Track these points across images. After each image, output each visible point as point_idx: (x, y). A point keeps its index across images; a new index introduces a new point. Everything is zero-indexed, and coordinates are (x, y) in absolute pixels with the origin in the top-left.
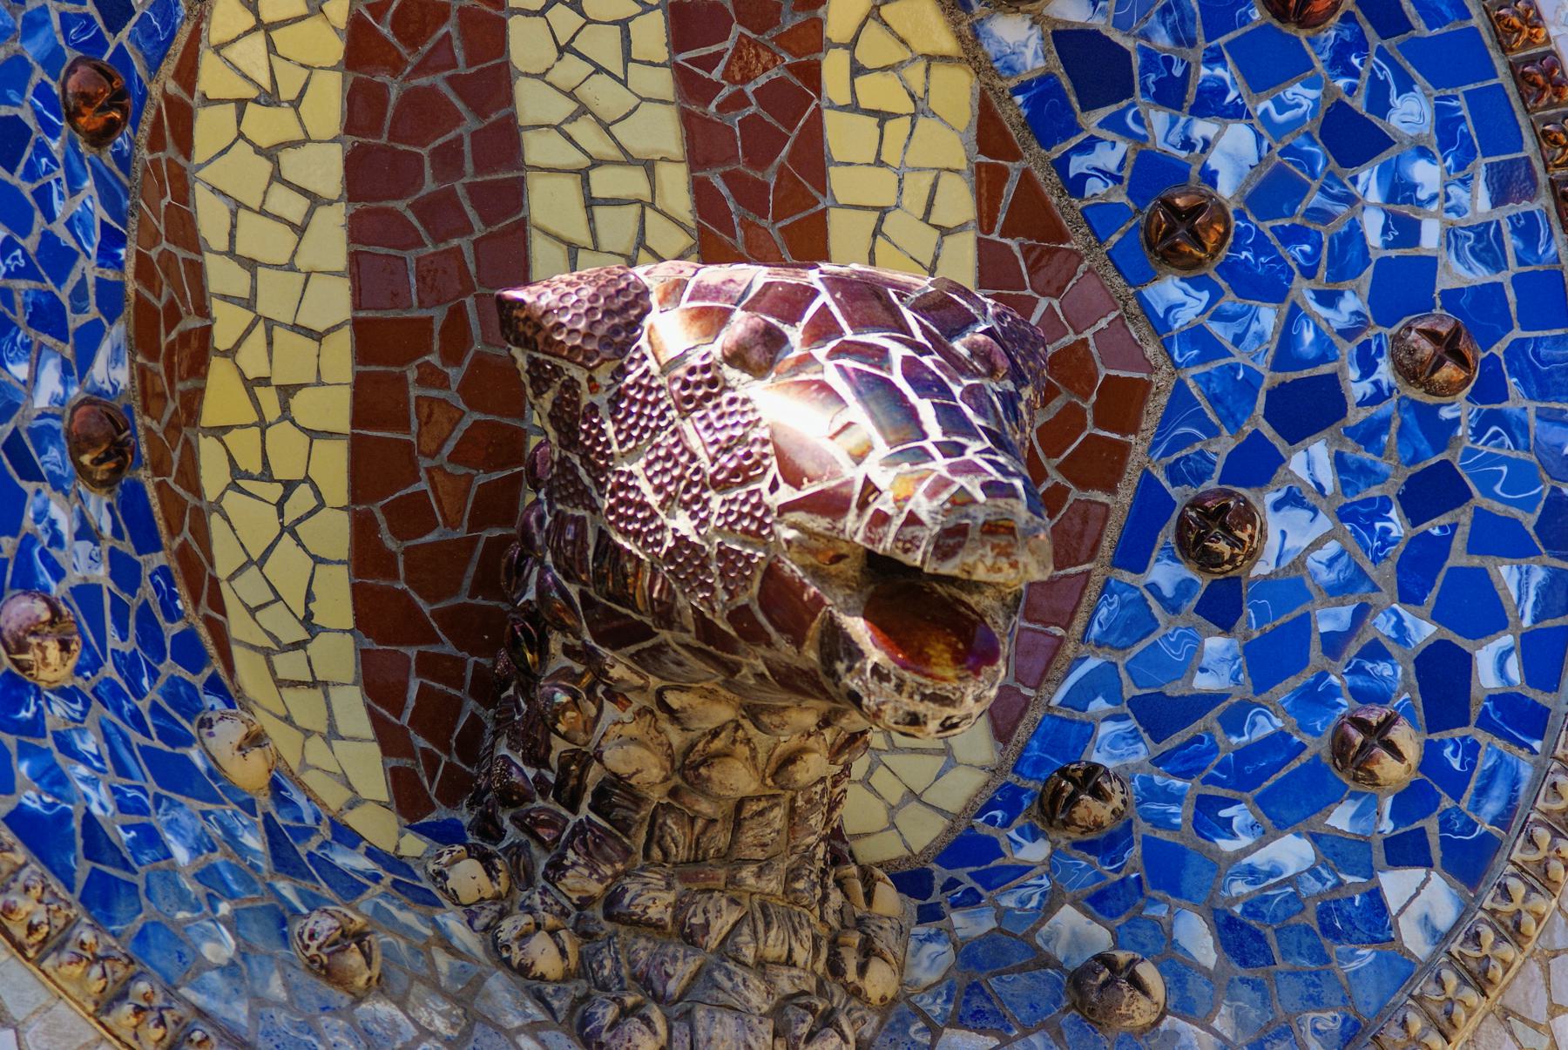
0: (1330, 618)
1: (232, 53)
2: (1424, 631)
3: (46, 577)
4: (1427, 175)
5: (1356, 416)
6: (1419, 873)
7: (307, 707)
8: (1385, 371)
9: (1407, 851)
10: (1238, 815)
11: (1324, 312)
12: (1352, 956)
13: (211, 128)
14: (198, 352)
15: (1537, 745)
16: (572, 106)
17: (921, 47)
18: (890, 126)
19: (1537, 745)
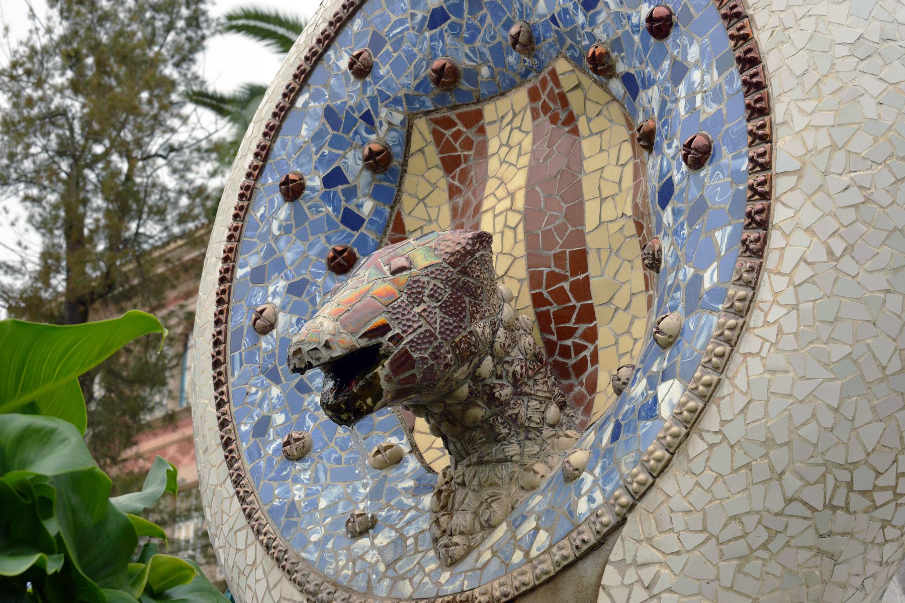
1: (413, 214)
2: (690, 271)
3: (310, 423)
5: (677, 190)
6: (671, 381)
8: (684, 168)
10: (638, 375)
11: (667, 151)
12: (644, 426)
15: (720, 307)
16: (499, 182)
17: (603, 102)
18: (604, 135)
19: (720, 307)
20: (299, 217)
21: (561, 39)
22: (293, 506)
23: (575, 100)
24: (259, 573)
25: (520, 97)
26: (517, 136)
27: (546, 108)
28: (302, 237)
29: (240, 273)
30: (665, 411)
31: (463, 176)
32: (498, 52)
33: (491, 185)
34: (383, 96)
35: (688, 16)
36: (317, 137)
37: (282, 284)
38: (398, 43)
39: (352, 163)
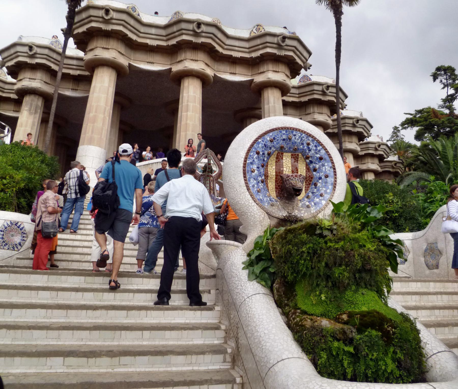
0: (321, 189)
4: (327, 167)
7: (272, 192)
9: (324, 200)
13: (269, 166)
14: (268, 176)
20: (259, 158)
21: (303, 152)
22: (261, 200)
23: (299, 159)
24: (255, 207)
25: (290, 154)
26: (288, 159)
27: (294, 158)
28: (259, 160)
29: (248, 162)
30: (323, 204)
31: (279, 160)
32: (290, 148)
33: (284, 164)
34: (274, 146)
35: (325, 159)
36: (263, 147)
37: (256, 166)
38: (278, 140)
39: (266, 153)
